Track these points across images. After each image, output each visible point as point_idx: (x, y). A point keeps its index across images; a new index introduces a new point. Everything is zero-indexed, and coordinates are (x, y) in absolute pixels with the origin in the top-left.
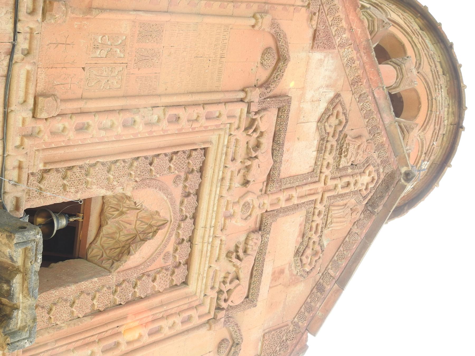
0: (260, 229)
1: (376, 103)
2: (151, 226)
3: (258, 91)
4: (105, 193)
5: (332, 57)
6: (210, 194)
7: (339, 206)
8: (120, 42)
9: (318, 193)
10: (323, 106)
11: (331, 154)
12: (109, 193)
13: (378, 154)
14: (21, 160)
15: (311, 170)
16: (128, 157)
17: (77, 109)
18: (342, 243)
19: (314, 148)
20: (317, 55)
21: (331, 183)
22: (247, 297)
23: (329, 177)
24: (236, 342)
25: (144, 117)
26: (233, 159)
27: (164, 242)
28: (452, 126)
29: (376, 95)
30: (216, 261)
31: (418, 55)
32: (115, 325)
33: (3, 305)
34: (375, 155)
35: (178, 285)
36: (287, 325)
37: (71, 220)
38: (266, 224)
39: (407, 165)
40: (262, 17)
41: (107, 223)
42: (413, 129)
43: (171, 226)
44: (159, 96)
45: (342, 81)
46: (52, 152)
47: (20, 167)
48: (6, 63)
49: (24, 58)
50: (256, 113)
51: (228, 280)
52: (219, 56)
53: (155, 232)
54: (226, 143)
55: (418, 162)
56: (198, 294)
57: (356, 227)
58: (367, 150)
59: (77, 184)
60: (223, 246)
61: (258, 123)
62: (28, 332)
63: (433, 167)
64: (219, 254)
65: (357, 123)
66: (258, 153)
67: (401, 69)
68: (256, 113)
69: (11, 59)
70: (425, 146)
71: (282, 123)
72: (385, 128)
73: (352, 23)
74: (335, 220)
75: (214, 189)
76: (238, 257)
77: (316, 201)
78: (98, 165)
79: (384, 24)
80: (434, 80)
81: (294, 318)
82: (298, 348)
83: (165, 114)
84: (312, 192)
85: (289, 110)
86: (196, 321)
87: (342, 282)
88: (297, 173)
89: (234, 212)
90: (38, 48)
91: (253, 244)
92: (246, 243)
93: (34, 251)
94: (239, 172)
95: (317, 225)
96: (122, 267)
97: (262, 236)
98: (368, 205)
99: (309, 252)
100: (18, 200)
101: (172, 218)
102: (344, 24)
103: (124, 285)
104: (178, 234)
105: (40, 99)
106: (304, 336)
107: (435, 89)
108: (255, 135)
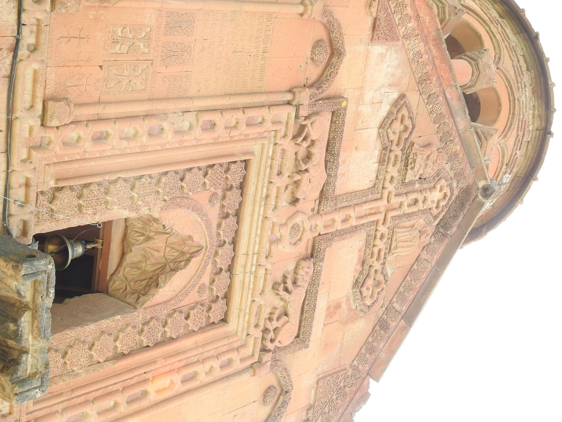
0: (312, 256)
1: (448, 104)
2: (183, 253)
3: (308, 92)
4: (128, 214)
6: (252, 215)
7: (405, 227)
8: (143, 35)
9: (380, 213)
10: (385, 109)
11: (395, 166)
12: (133, 215)
13: (451, 165)
14: (29, 176)
15: (371, 185)
16: (155, 172)
17: (94, 115)
18: (409, 272)
19: (375, 159)
20: (378, 49)
21: (395, 201)
22: (298, 336)
23: (393, 193)
25: (173, 124)
26: (280, 173)
27: (199, 272)
28: (538, 132)
29: (448, 96)
30: (260, 294)
31: (497, 48)
32: (142, 371)
33: (10, 348)
34: (448, 167)
35: (216, 322)
36: (346, 369)
37: (89, 247)
38: (319, 250)
39: (485, 179)
40: (312, 4)
41: (131, 251)
42: (492, 135)
43: (207, 254)
44: (191, 98)
45: (408, 78)
46: (65, 167)
47: (27, 185)
48: (8, 61)
49: (30, 55)
50: (306, 118)
51: (275, 317)
52: (261, 51)
53: (188, 261)
54: (270, 154)
55: (498, 175)
56: (239, 334)
57: (425, 253)
58: (438, 161)
59: (95, 204)
60: (268, 276)
61: (309, 130)
62: (40, 380)
63: (516, 180)
64: (264, 286)
65: (425, 129)
67: (477, 64)
68: (306, 118)
69: (15, 57)
70: (506, 156)
71: (337, 130)
72: (459, 135)
73: (419, 10)
74: (400, 244)
75: (257, 209)
76: (286, 290)
77: (377, 222)
78: (120, 181)
79: (456, 11)
80: (516, 77)
81: (353, 361)
82: (358, 396)
83: (198, 120)
84: (373, 211)
85: (345, 114)
86: (237, 366)
87: (410, 317)
88: (356, 189)
89: (281, 236)
90: (47, 42)
91: (303, 274)
92: (295, 273)
93: (46, 284)
94: (286, 188)
95: (380, 251)
96: (149, 302)
97: (314, 264)
98: (439, 226)
99: (370, 282)
100: (25, 224)
101: (208, 244)
102: (409, 10)
103: (151, 324)
104: (215, 263)
105: (50, 104)
106: (365, 382)
107: (518, 87)
108: (305, 144)
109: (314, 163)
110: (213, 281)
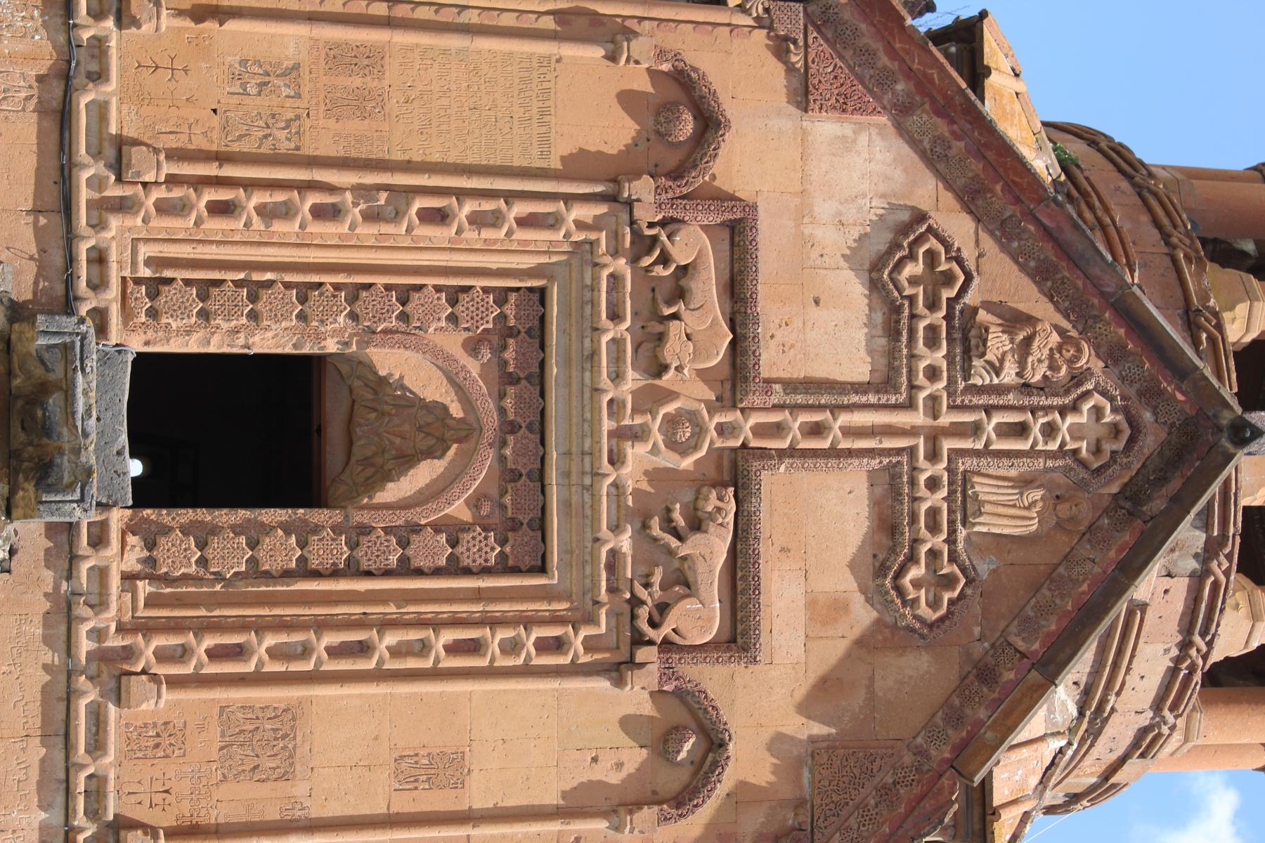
5: (880, 134)
6: (569, 385)
15: (878, 378)
24: (717, 742)
29: (1046, 221)
50: (651, 225)
52: (535, 110)
54: (588, 282)
66: (680, 307)
73: (907, 58)
75: (575, 373)
77: (912, 451)
82: (928, 805)
99: (917, 572)
102: (884, 60)
104: (502, 459)
105: (124, 148)
106: (945, 781)
109: (692, 307)
110: (503, 493)
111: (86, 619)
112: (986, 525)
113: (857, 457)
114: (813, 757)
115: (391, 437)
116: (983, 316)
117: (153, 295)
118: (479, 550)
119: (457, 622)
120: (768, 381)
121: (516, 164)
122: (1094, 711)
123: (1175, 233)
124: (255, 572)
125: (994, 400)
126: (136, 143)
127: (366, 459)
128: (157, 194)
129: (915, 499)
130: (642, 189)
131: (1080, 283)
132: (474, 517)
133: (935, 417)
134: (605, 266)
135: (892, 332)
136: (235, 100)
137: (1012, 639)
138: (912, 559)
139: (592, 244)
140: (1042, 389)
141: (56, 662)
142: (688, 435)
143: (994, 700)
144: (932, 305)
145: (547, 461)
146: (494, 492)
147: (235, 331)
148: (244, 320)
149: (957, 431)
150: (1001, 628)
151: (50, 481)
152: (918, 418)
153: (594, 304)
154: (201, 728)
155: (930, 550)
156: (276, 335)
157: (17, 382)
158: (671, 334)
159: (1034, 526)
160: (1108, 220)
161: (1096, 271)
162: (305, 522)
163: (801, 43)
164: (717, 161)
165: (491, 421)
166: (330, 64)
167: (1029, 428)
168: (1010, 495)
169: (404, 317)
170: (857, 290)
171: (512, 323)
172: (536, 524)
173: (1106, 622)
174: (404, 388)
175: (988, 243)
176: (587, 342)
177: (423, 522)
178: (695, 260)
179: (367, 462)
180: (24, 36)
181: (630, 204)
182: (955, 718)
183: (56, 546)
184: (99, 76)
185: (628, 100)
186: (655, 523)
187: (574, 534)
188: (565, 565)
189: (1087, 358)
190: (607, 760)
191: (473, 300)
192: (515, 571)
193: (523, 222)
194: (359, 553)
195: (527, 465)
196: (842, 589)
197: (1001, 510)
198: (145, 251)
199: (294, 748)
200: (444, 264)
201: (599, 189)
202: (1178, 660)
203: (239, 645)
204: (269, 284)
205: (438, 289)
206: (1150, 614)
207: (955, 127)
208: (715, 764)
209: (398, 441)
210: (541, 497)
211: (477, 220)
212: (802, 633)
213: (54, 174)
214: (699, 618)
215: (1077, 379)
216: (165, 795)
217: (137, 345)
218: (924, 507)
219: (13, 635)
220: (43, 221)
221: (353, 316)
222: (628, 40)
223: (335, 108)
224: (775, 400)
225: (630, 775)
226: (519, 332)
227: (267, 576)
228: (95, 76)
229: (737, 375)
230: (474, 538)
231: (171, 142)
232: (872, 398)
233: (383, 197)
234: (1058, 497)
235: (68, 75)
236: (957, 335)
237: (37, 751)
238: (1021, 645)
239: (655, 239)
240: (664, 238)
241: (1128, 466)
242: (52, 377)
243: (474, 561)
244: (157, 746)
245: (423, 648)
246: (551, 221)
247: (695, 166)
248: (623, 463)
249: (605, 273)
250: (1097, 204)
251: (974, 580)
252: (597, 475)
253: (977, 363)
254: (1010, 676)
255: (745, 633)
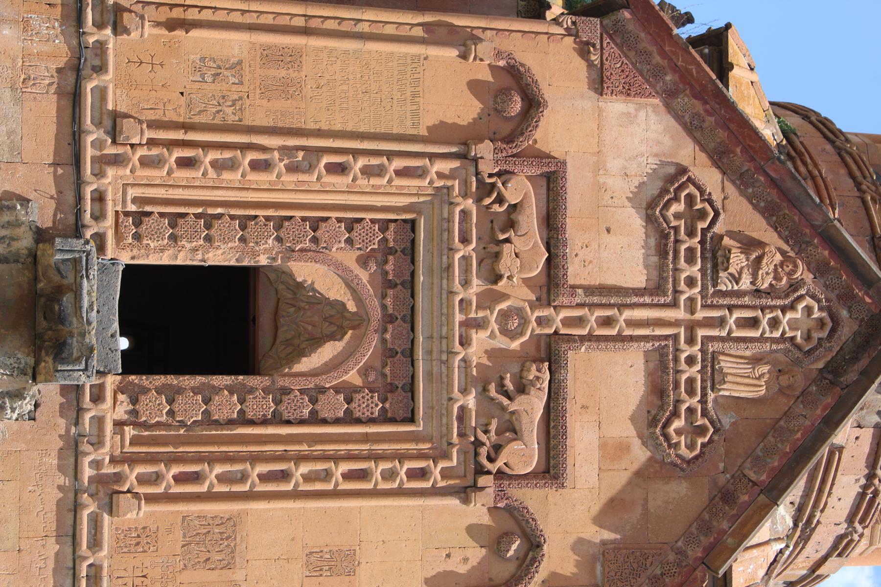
5: (654, 111)
6: (432, 289)
15: (652, 285)
24: (535, 543)
29: (772, 174)
50: (491, 176)
52: (409, 94)
54: (446, 215)
64: (466, 383)
75: (436, 281)
77: (676, 337)
99: (679, 423)
102: (657, 59)
104: (384, 341)
105: (118, 120)
106: (698, 574)
109: (519, 234)
111: (89, 454)
112: (729, 390)
113: (637, 341)
114: (604, 555)
115: (306, 325)
116: (727, 241)
117: (138, 224)
118: (367, 406)
119: (351, 457)
120: (573, 287)
121: (395, 132)
122: (804, 524)
123: (865, 182)
124: (208, 421)
125: (734, 301)
126: (126, 116)
127: (287, 340)
128: (141, 152)
129: (678, 372)
130: (484, 149)
131: (796, 218)
132: (363, 383)
133: (693, 313)
134: (458, 204)
135: (662, 253)
136: (197, 86)
137: (746, 472)
138: (675, 414)
139: (449, 189)
140: (769, 293)
141: (67, 484)
142: (516, 325)
143: (733, 516)
144: (691, 234)
145: (415, 343)
146: (378, 364)
147: (195, 250)
148: (201, 242)
149: (708, 323)
150: (739, 464)
151: (64, 355)
152: (680, 314)
153: (450, 231)
154: (169, 531)
155: (688, 408)
156: (224, 253)
157: (41, 285)
158: (505, 253)
159: (762, 391)
160: (817, 173)
161: (808, 209)
162: (244, 385)
163: (598, 47)
164: (538, 130)
165: (376, 314)
166: (264, 61)
167: (759, 324)
168: (746, 369)
169: (315, 240)
170: (636, 222)
171: (391, 244)
172: (408, 387)
173: (814, 460)
174: (314, 290)
175: (731, 189)
176: (445, 258)
177: (327, 386)
178: (522, 200)
179: (288, 342)
180: (48, 41)
181: (476, 160)
182: (706, 528)
183: (67, 402)
184: (101, 69)
185: (475, 86)
186: (492, 387)
187: (434, 394)
188: (428, 417)
189: (802, 272)
190: (457, 556)
191: (364, 228)
192: (393, 421)
193: (399, 173)
194: (282, 408)
195: (401, 345)
196: (625, 435)
197: (739, 380)
198: (132, 193)
199: (235, 546)
200: (344, 202)
201: (454, 149)
202: (865, 487)
203: (196, 473)
204: (220, 216)
205: (339, 220)
206: (845, 453)
207: (708, 106)
208: (534, 560)
209: (310, 328)
210: (411, 369)
211: (367, 172)
212: (596, 466)
213: (68, 138)
214: (523, 456)
215: (794, 286)
216: (143, 579)
217: (125, 259)
218: (684, 377)
219: (37, 464)
220: (60, 171)
221: (279, 239)
222: (475, 44)
223: (267, 91)
224: (578, 300)
225: (473, 567)
226: (396, 251)
227: (217, 423)
228: (98, 69)
229: (551, 282)
230: (363, 397)
231: (151, 116)
232: (647, 300)
233: (301, 154)
234: (780, 371)
235: (79, 67)
236: (709, 255)
237: (53, 547)
238: (752, 476)
239: (493, 185)
240: (500, 185)
241: (830, 349)
242: (65, 282)
243: (363, 414)
244: (138, 544)
245: (327, 475)
246: (420, 172)
247: (522, 134)
248: (470, 344)
249: (458, 210)
250: (809, 161)
251: (719, 430)
252: (451, 353)
253: (722, 274)
254: (745, 498)
255: (556, 466)
